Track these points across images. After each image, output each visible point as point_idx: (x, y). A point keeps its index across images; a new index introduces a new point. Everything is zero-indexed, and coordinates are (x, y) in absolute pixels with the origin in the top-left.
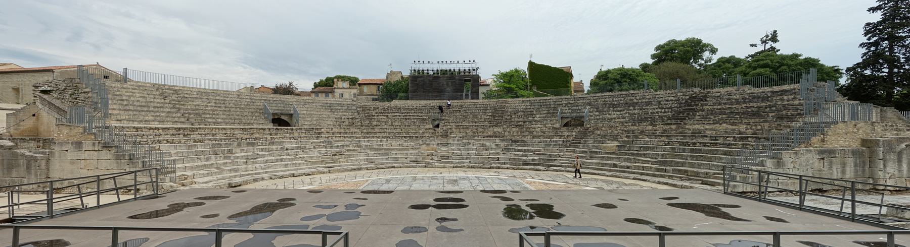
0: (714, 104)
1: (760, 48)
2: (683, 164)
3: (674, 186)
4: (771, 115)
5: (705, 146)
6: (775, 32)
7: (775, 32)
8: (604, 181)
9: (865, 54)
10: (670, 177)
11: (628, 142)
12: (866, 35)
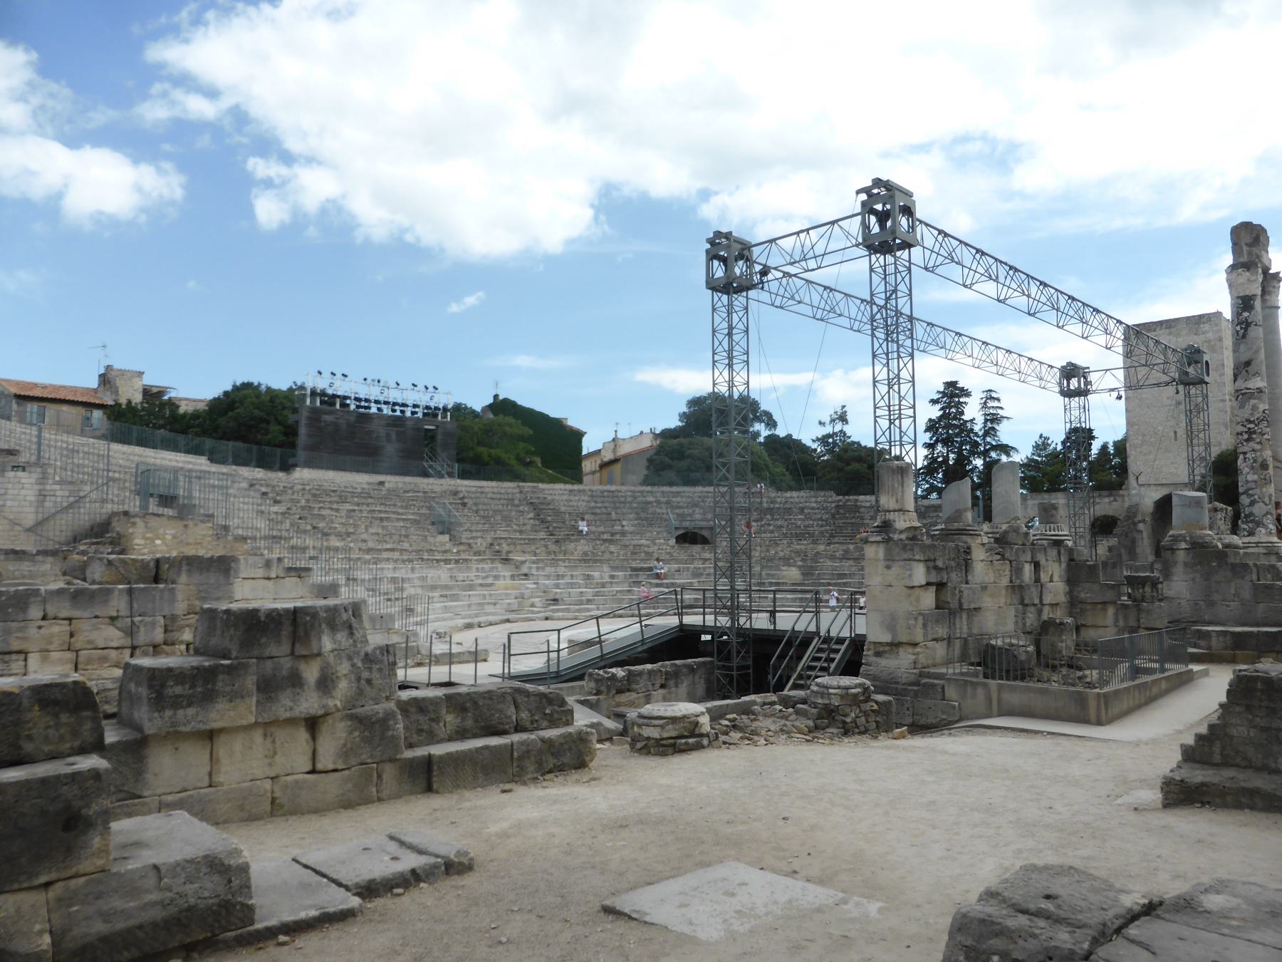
1: (828, 430)
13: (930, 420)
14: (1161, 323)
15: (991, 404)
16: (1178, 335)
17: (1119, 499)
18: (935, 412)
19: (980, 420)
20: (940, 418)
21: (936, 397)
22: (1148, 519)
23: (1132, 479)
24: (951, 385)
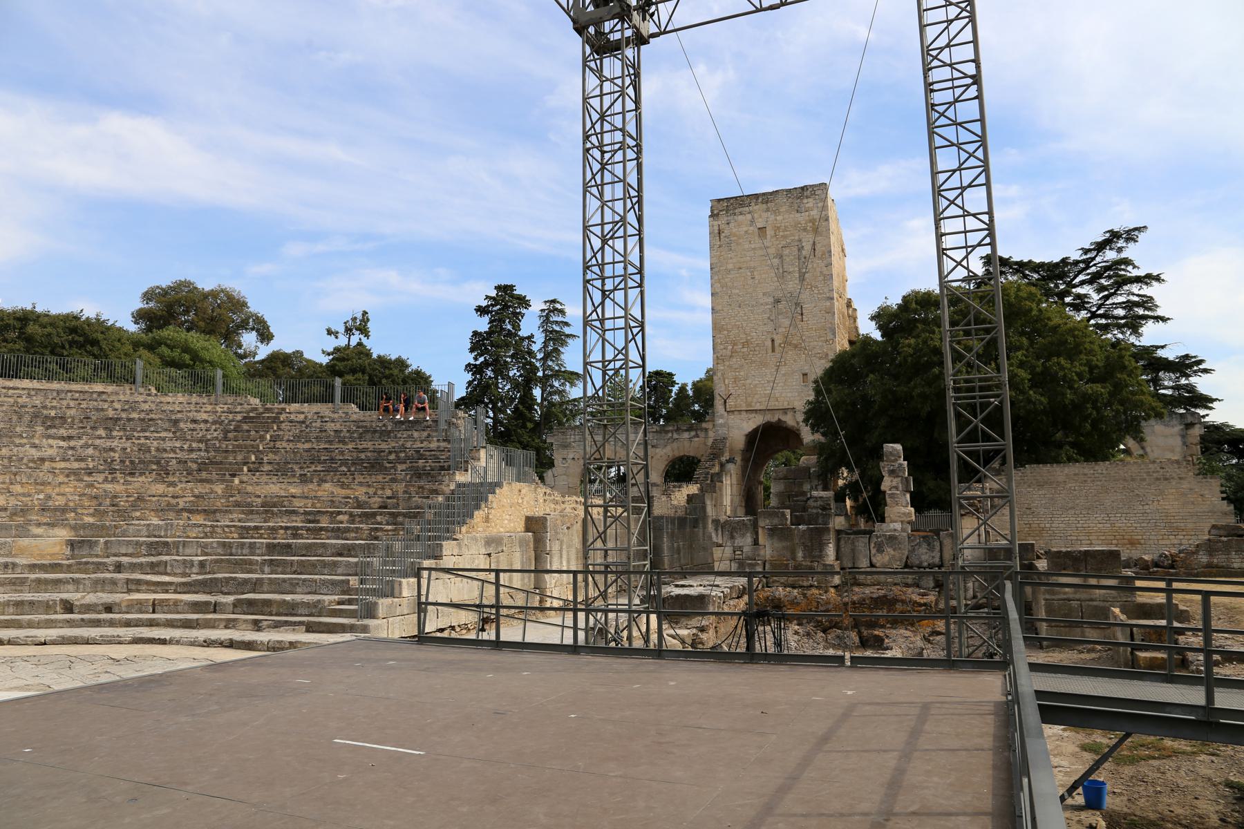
0: (297, 439)
1: (342, 341)
2: (256, 586)
3: (249, 646)
4: (400, 467)
5: (295, 536)
6: (365, 313)
7: (365, 313)
8: (38, 662)
9: (470, 383)
10: (229, 624)
11: (101, 530)
12: (472, 350)
13: (475, 333)
14: (756, 196)
15: (554, 318)
16: (776, 212)
17: (702, 434)
18: (483, 324)
19: (539, 338)
20: (490, 333)
21: (484, 303)
22: (738, 459)
23: (718, 403)
24: (506, 290)
